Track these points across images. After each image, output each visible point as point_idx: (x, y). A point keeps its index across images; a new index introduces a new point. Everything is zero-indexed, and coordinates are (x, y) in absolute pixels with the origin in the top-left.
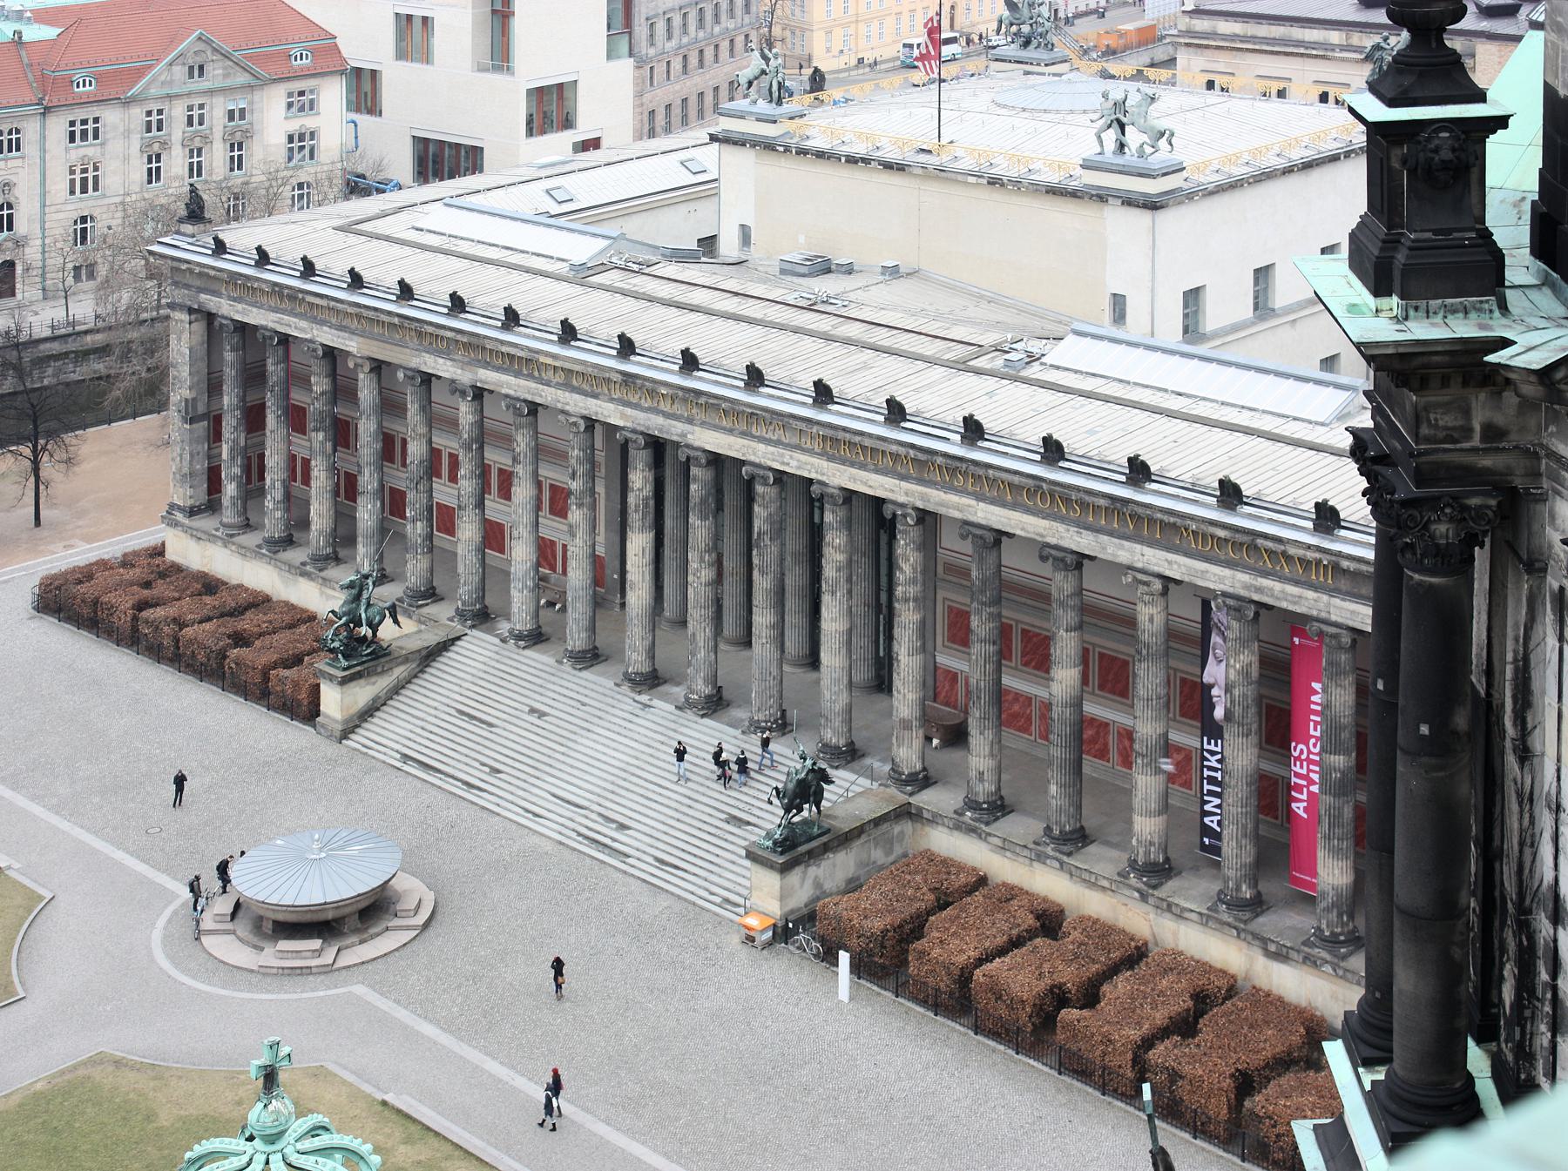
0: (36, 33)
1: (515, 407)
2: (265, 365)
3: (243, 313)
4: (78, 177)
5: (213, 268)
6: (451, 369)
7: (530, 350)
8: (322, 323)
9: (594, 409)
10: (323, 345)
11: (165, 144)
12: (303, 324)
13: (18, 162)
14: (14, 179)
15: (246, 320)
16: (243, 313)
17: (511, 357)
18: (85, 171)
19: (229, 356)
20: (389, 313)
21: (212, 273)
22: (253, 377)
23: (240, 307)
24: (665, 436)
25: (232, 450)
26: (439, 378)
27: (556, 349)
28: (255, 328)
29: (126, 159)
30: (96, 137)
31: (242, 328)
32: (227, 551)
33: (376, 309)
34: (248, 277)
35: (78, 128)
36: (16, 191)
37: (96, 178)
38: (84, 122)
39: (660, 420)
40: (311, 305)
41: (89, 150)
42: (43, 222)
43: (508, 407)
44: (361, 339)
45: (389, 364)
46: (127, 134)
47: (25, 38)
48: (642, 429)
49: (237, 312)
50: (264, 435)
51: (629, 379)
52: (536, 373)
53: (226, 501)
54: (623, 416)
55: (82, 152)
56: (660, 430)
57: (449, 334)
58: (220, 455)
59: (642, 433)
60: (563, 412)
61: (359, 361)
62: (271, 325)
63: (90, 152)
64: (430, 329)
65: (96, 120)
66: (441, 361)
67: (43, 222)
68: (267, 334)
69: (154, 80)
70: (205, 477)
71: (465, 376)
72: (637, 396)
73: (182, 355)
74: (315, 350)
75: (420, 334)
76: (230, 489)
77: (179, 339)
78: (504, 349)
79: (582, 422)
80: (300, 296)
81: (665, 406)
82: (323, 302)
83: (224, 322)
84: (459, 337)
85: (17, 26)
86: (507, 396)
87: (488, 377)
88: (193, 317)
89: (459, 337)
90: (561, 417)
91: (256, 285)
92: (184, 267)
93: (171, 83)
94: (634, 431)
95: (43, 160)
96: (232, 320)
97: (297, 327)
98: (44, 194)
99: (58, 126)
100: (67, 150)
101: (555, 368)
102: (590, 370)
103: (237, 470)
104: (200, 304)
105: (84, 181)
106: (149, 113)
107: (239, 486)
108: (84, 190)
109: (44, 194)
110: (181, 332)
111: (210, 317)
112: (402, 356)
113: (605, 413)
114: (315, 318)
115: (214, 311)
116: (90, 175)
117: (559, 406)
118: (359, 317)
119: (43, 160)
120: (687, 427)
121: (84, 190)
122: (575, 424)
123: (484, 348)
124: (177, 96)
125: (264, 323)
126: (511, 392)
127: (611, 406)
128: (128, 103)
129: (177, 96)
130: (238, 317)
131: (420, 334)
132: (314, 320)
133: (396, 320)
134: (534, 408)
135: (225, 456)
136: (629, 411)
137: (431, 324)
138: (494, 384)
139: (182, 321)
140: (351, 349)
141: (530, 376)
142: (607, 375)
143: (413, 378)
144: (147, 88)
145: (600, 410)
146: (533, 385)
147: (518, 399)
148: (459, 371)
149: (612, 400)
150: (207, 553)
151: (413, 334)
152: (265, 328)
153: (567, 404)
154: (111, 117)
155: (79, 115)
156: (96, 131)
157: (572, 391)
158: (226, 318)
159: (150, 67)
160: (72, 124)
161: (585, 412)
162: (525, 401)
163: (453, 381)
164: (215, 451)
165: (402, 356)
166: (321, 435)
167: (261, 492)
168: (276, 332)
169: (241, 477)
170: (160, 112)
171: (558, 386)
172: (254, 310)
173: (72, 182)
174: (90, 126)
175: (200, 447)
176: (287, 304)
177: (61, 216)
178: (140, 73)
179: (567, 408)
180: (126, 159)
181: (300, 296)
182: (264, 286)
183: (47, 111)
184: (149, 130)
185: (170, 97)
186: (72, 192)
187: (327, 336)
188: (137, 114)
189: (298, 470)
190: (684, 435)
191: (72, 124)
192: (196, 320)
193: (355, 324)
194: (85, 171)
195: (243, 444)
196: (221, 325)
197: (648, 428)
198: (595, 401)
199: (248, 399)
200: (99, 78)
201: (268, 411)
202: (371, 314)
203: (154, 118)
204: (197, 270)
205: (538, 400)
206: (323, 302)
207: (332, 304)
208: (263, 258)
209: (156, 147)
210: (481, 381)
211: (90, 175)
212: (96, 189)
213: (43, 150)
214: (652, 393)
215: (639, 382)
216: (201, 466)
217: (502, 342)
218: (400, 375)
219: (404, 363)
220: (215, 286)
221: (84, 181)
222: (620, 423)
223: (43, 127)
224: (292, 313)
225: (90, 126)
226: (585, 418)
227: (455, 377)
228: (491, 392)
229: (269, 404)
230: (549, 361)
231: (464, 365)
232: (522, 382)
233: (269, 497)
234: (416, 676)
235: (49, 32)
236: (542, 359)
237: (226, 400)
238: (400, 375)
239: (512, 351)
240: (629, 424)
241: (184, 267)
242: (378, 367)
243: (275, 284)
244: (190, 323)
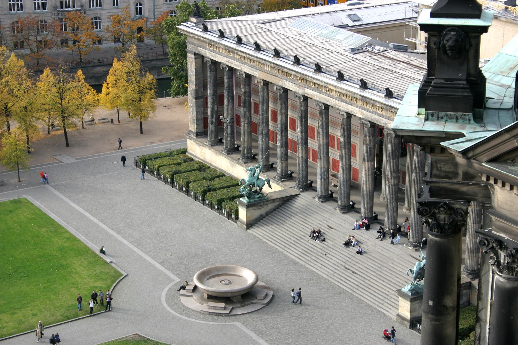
1: (319, 106)
2: (223, 79)
3: (215, 56)
5: (203, 37)
6: (295, 88)
7: (325, 83)
8: (245, 64)
9: (350, 109)
10: (245, 73)
12: (238, 63)
15: (216, 59)
16: (215, 56)
17: (318, 85)
19: (209, 74)
20: (270, 62)
21: (202, 39)
22: (218, 83)
23: (213, 54)
24: (378, 123)
25: (211, 111)
26: (291, 91)
27: (335, 83)
28: (219, 63)
31: (215, 63)
32: (210, 151)
33: (265, 60)
34: (216, 42)
39: (377, 117)
40: (241, 56)
43: (317, 106)
44: (260, 72)
45: (272, 83)
48: (370, 120)
49: (213, 56)
50: (223, 107)
51: (364, 99)
52: (328, 92)
53: (209, 132)
54: (362, 113)
56: (377, 121)
57: (293, 73)
58: (207, 113)
59: (369, 122)
60: (338, 109)
61: (259, 81)
62: (225, 63)
64: (286, 70)
66: (291, 84)
68: (224, 66)
70: (202, 121)
71: (300, 91)
72: (368, 106)
73: (192, 71)
74: (242, 75)
75: (282, 72)
76: (211, 127)
77: (191, 66)
78: (315, 81)
79: (345, 114)
80: (236, 52)
81: (379, 111)
82: (245, 55)
83: (208, 60)
84: (297, 75)
86: (316, 101)
87: (309, 92)
88: (196, 56)
89: (297, 75)
90: (338, 111)
91: (219, 46)
92: (192, 35)
94: (366, 120)
96: (211, 59)
97: (235, 64)
101: (335, 91)
102: (349, 93)
103: (214, 120)
104: (198, 51)
107: (215, 126)
110: (192, 62)
111: (203, 57)
112: (276, 80)
113: (355, 111)
114: (242, 61)
115: (204, 55)
117: (337, 107)
118: (259, 63)
120: (387, 121)
122: (343, 115)
123: (307, 80)
125: (223, 61)
126: (318, 99)
127: (357, 109)
130: (213, 58)
131: (282, 72)
132: (242, 62)
133: (273, 65)
134: (327, 107)
135: (209, 114)
136: (364, 112)
137: (286, 68)
138: (312, 95)
139: (192, 58)
140: (256, 76)
141: (325, 94)
142: (355, 96)
143: (280, 90)
145: (353, 110)
146: (327, 97)
147: (320, 102)
148: (298, 89)
149: (357, 107)
150: (203, 151)
151: (280, 71)
152: (223, 64)
153: (340, 106)
157: (342, 101)
158: (208, 58)
161: (347, 111)
162: (324, 104)
163: (295, 92)
164: (206, 111)
165: (276, 80)
166: (245, 109)
167: (222, 130)
168: (227, 66)
169: (216, 123)
171: (336, 99)
172: (219, 56)
175: (200, 109)
176: (231, 55)
179: (340, 108)
181: (236, 52)
182: (222, 46)
187: (247, 69)
189: (236, 120)
190: (386, 124)
192: (198, 58)
193: (257, 65)
195: (216, 110)
196: (206, 61)
197: (372, 119)
198: (351, 106)
199: (218, 92)
201: (225, 97)
202: (263, 62)
204: (197, 37)
205: (328, 103)
206: (245, 55)
207: (248, 56)
208: (222, 35)
210: (306, 93)
214: (373, 105)
215: (368, 100)
216: (201, 117)
217: (314, 78)
218: (275, 88)
219: (277, 83)
220: (204, 44)
222: (361, 116)
224: (233, 58)
226: (346, 113)
227: (296, 91)
228: (311, 99)
229: (225, 95)
230: (332, 88)
231: (300, 86)
232: (323, 96)
233: (225, 132)
234: (280, 206)
236: (330, 87)
237: (209, 91)
238: (275, 88)
239: (318, 82)
240: (364, 117)
241: (192, 35)
242: (266, 84)
243: (226, 46)
244: (195, 59)
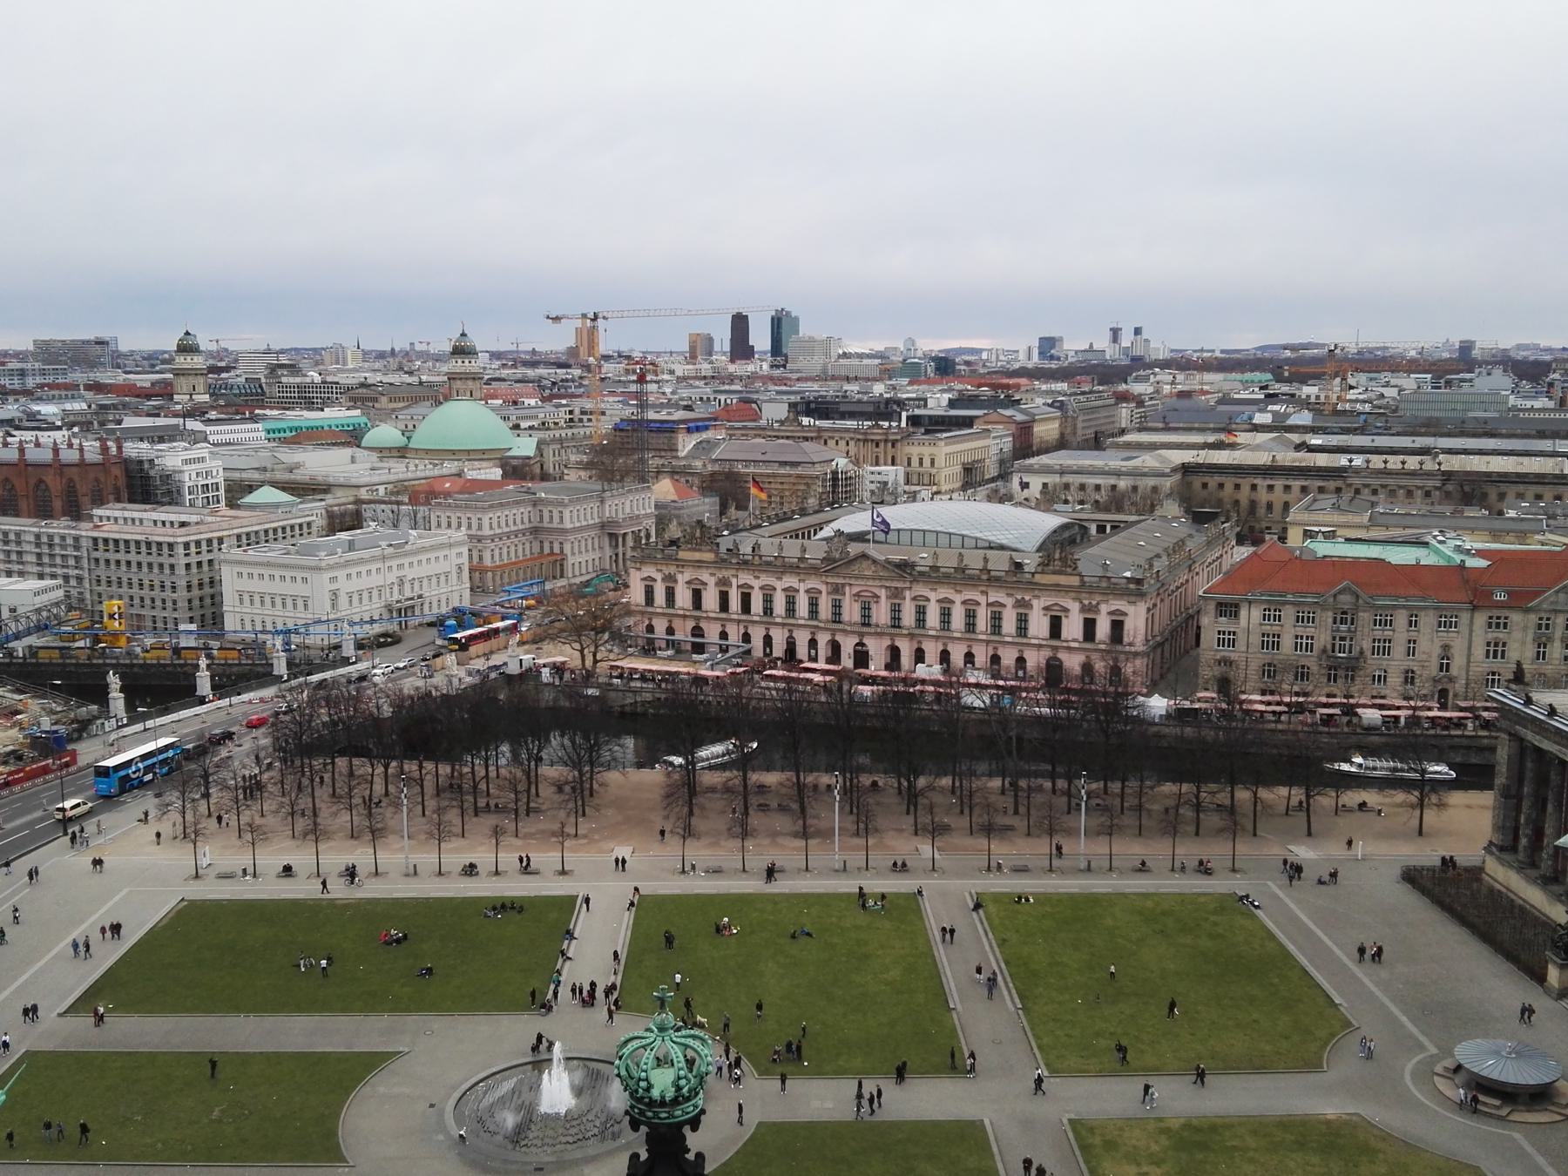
0: (1472, 563)
4: (1492, 649)
11: (1550, 639)
13: (1455, 635)
14: (1452, 643)
18: (1496, 645)
29: (1523, 643)
30: (1505, 628)
35: (1494, 621)
36: (1452, 651)
37: (1503, 652)
38: (1498, 618)
41: (1501, 635)
42: (1468, 671)
46: (1525, 629)
47: (1467, 565)
55: (1495, 635)
63: (1501, 635)
65: (1506, 618)
67: (1468, 671)
69: (1546, 599)
85: (1463, 557)
93: (1557, 602)
95: (1470, 635)
98: (1469, 655)
99: (1481, 619)
100: (1486, 632)
105: (1495, 652)
106: (1541, 619)
108: (1495, 657)
109: (1469, 655)
116: (1500, 649)
119: (1470, 635)
121: (1495, 657)
124: (1560, 611)
128: (1527, 611)
129: (1560, 611)
144: (1541, 602)
154: (1516, 617)
155: (1496, 613)
156: (1505, 624)
159: (1545, 592)
160: (1491, 618)
170: (1548, 619)
173: (1488, 651)
174: (1502, 621)
177: (1480, 669)
178: (1537, 594)
180: (1523, 643)
183: (1475, 608)
184: (1540, 628)
185: (1556, 611)
186: (1488, 657)
188: (1533, 618)
191: (1491, 618)
194: (1496, 645)
200: (1509, 594)
203: (1544, 622)
209: (1544, 639)
211: (1500, 649)
212: (1503, 657)
213: (1471, 631)
221: (1495, 652)
223: (1472, 618)
225: (1502, 621)
235: (1483, 563)
